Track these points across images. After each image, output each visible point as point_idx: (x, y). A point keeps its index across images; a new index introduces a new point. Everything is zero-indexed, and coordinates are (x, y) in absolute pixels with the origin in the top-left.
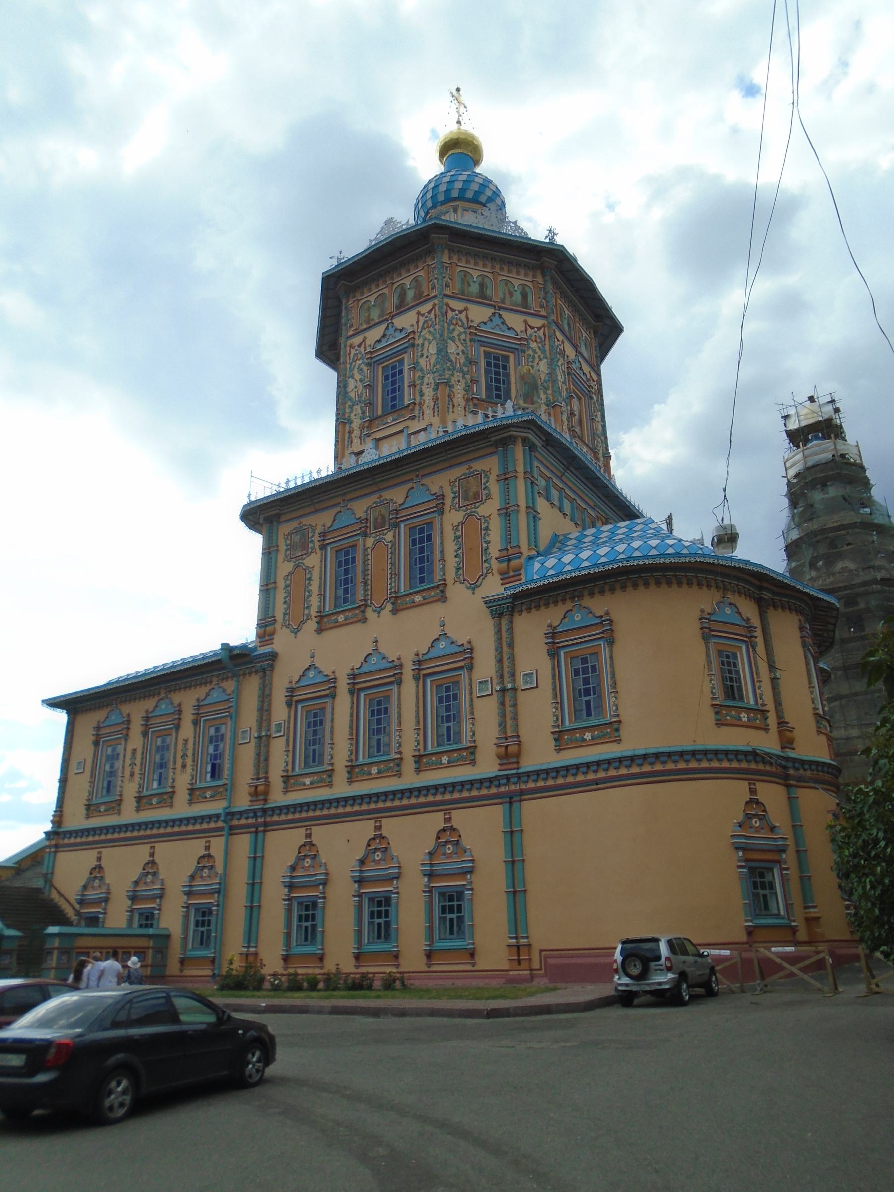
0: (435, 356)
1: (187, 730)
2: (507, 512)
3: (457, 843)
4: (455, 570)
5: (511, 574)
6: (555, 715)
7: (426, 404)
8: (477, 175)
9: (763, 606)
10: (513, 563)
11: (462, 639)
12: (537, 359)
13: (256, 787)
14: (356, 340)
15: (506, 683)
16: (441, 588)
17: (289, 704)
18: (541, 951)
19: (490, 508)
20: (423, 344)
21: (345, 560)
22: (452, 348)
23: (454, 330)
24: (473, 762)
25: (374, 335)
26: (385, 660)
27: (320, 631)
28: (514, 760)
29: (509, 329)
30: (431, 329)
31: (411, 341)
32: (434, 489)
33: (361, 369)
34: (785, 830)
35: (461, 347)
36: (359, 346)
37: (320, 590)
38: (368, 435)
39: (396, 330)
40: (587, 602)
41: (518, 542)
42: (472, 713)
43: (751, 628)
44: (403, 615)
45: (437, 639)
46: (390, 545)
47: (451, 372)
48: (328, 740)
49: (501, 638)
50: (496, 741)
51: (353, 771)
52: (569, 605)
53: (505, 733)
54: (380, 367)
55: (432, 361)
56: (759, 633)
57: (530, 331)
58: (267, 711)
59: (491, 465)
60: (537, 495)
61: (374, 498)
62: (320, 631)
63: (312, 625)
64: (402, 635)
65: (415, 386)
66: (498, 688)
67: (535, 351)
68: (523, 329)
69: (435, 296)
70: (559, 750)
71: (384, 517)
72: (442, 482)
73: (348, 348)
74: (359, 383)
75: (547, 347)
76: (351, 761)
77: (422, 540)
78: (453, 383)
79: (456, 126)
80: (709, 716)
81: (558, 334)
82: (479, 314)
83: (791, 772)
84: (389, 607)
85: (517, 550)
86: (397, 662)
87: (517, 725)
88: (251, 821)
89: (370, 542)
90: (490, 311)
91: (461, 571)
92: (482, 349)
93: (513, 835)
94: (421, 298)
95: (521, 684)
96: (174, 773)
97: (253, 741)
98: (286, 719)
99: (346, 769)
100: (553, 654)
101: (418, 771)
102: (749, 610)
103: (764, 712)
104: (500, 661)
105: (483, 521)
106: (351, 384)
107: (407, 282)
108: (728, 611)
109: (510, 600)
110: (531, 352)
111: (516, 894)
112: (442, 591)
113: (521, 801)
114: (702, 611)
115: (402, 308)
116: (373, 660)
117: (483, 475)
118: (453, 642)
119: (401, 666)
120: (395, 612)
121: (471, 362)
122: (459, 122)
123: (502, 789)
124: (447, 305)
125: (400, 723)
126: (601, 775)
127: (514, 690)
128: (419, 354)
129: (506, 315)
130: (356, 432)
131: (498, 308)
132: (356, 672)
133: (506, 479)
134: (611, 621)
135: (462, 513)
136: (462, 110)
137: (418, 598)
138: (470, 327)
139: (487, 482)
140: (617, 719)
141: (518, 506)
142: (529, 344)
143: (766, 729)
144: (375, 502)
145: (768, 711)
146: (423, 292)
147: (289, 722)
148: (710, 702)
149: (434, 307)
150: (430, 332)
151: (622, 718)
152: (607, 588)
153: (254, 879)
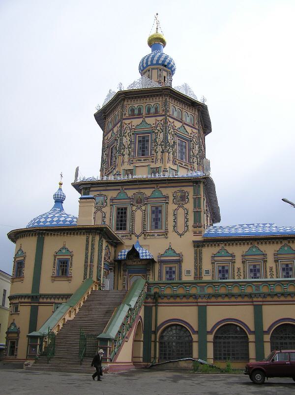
14: (127, 122)
35: (172, 138)
36: (129, 124)
54: (137, 136)
55: (161, 141)
71: (141, 200)
72: (169, 192)
77: (157, 211)
82: (178, 125)
84: (143, 235)
89: (134, 208)
130: (126, 160)
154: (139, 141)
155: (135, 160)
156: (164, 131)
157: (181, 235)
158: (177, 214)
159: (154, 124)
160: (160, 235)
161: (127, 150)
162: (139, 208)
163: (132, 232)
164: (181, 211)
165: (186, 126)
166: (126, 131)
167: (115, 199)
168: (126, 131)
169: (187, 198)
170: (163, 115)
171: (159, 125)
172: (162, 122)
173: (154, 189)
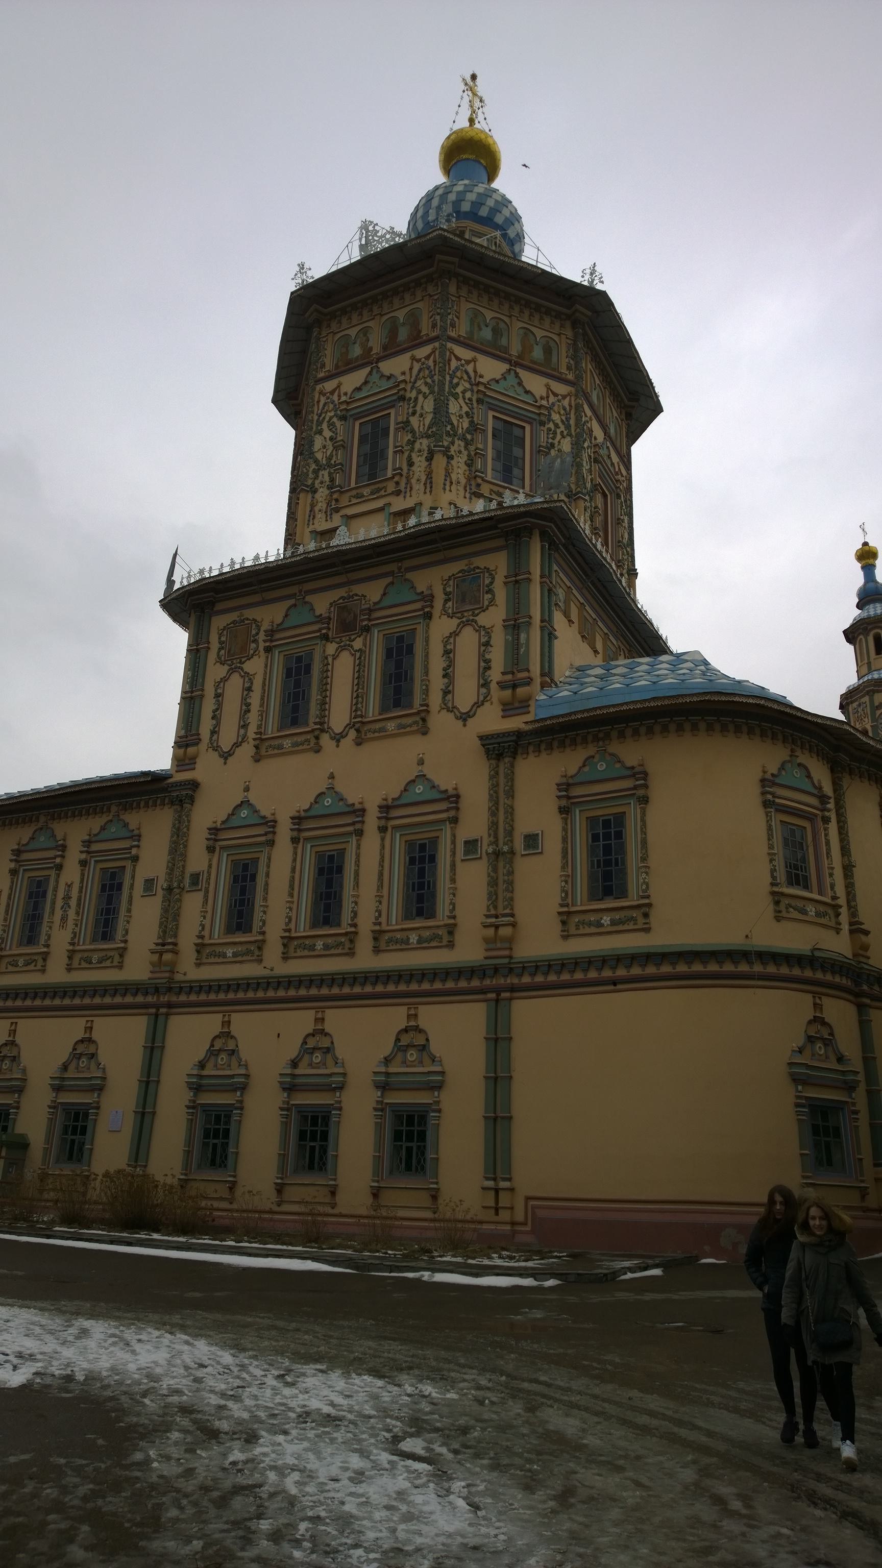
0: (431, 415)
1: (71, 873)
2: (516, 625)
3: (424, 1048)
4: (441, 694)
5: (517, 705)
6: (563, 890)
7: (416, 477)
8: (495, 191)
9: (835, 768)
10: (519, 690)
11: (446, 783)
12: (559, 437)
13: (161, 954)
15: (501, 842)
16: (423, 715)
17: (211, 850)
18: (528, 1199)
19: (494, 617)
20: (416, 399)
21: (298, 672)
22: (454, 407)
23: (458, 384)
24: (451, 945)
25: (351, 381)
26: (341, 803)
27: (257, 759)
28: (507, 945)
29: (527, 392)
30: (429, 380)
31: (401, 393)
32: (421, 587)
33: (333, 424)
34: (856, 1063)
37: (262, 705)
38: (337, 510)
39: (382, 376)
40: (615, 747)
41: (528, 664)
42: (453, 880)
43: (823, 799)
44: (367, 747)
45: (413, 781)
46: (358, 655)
47: (450, 439)
48: (259, 901)
49: (498, 785)
50: (484, 920)
51: (290, 944)
52: (591, 750)
53: (495, 907)
55: (428, 419)
56: (831, 806)
57: (552, 399)
58: (182, 855)
59: (498, 563)
60: (553, 608)
61: (342, 592)
62: (257, 759)
63: (247, 750)
64: (370, 773)
65: (403, 452)
66: (490, 850)
67: (557, 426)
68: (544, 395)
69: (436, 339)
70: (565, 937)
72: (432, 579)
75: (572, 422)
76: (289, 931)
78: (453, 453)
79: (468, 124)
80: (766, 906)
81: (586, 407)
82: (490, 368)
83: (865, 987)
84: (352, 734)
85: (525, 674)
86: (358, 806)
87: (512, 899)
88: (150, 999)
89: (331, 648)
90: (505, 367)
91: (450, 696)
92: (491, 414)
93: (498, 1042)
94: (417, 341)
95: (519, 844)
96: (50, 928)
97: (160, 893)
98: (206, 868)
99: (280, 942)
100: (564, 811)
101: (377, 950)
102: (821, 774)
103: (836, 907)
104: (493, 813)
105: (483, 633)
106: (318, 442)
107: (401, 315)
108: (797, 773)
109: (514, 738)
110: (551, 425)
111: (498, 1121)
112: (424, 720)
113: (511, 999)
114: (764, 772)
115: (391, 349)
116: (328, 801)
117: (487, 575)
118: (434, 787)
119: (364, 810)
120: (359, 743)
121: (474, 428)
122: (471, 121)
123: (487, 982)
124: (452, 353)
125: (357, 884)
126: (621, 972)
127: (512, 852)
128: (411, 410)
129: (522, 373)
130: (322, 505)
131: (515, 364)
132: (303, 814)
133: (516, 582)
134: (645, 775)
135: (456, 621)
136: (477, 104)
137: (391, 726)
138: (478, 384)
139: (492, 583)
140: (646, 901)
141: (530, 617)
142: (550, 415)
143: (838, 931)
144: (342, 598)
145: (841, 907)
146: (420, 332)
147: (209, 873)
148: (768, 888)
149: (433, 352)
150: (426, 384)
151: (654, 900)
152: (643, 730)
153: (149, 1076)
154: (363, 439)
155: (344, 501)
156: (436, 389)
157: (464, 718)
158: (458, 653)
160: (404, 727)
161: (326, 473)
162: (341, 649)
163: (323, 727)
164: (468, 641)
165: (518, 370)
167: (280, 628)
168: (323, 415)
169: (490, 591)
170: (436, 339)
173: (390, 579)
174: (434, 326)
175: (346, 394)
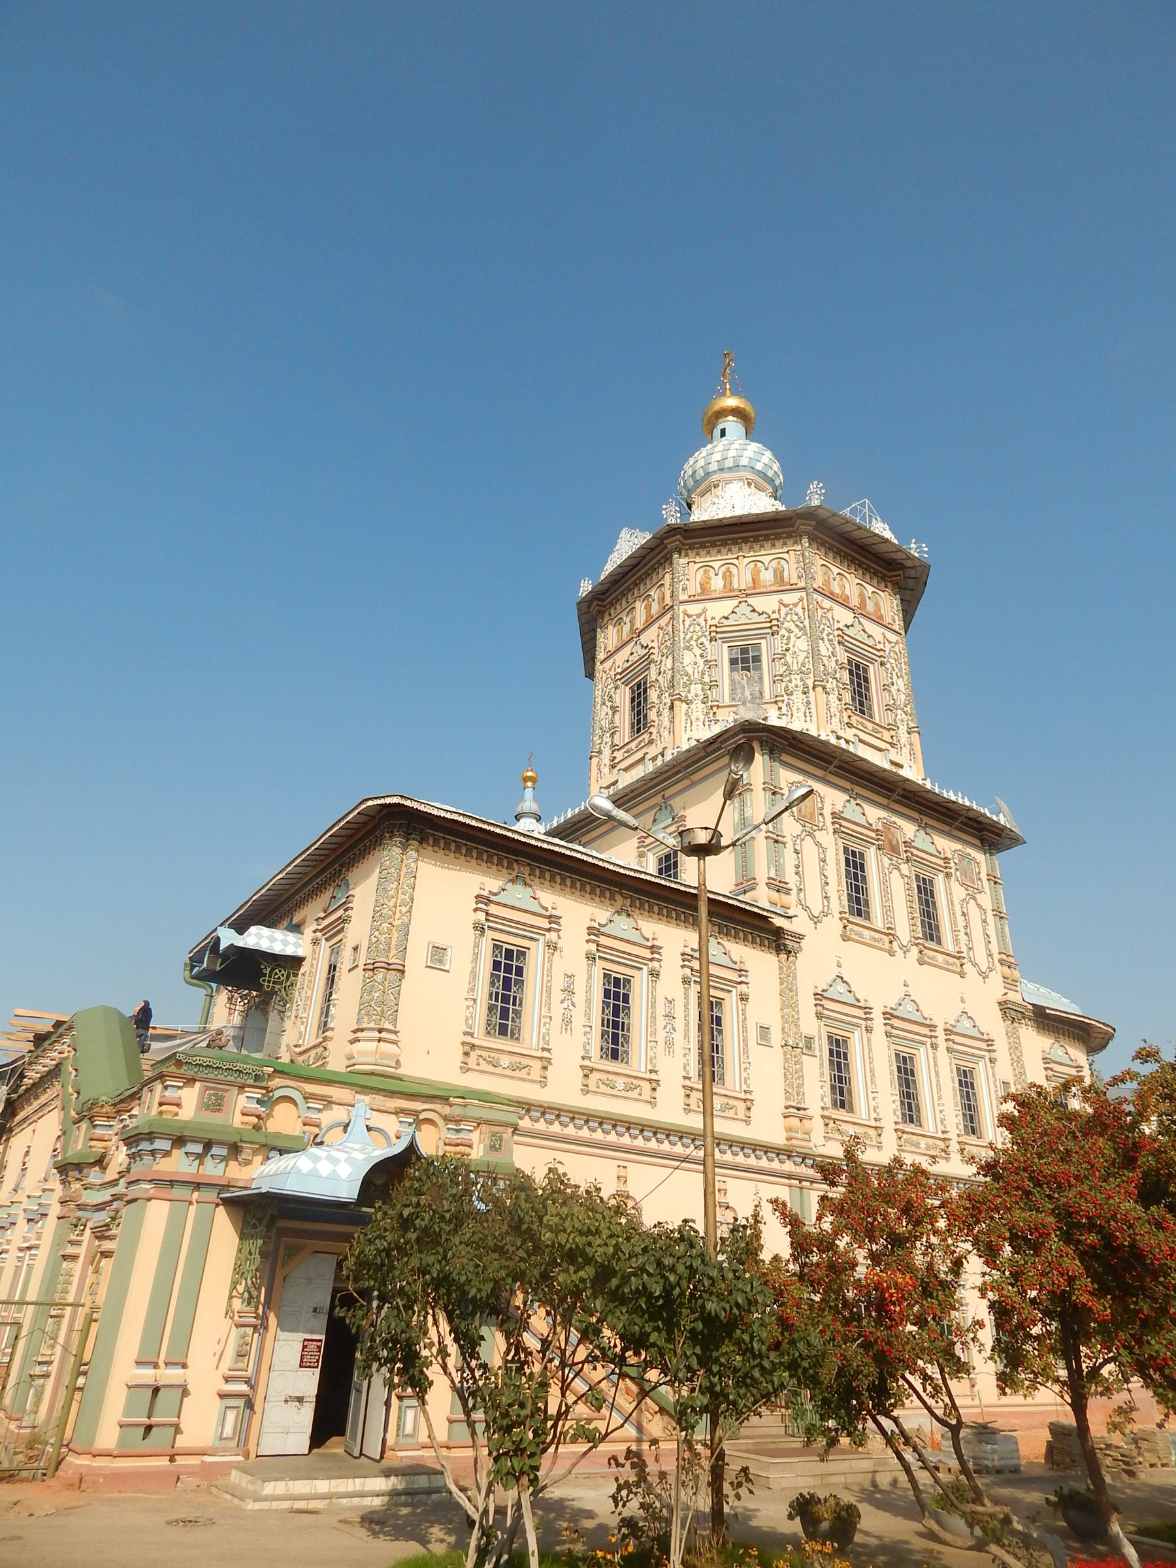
14: (693, 609)
20: (789, 638)
31: (775, 628)
36: (699, 616)
73: (682, 615)
74: (701, 662)
159: (774, 612)
166: (690, 635)
171: (788, 618)
172: (799, 609)
174: (799, 577)
175: (713, 618)
